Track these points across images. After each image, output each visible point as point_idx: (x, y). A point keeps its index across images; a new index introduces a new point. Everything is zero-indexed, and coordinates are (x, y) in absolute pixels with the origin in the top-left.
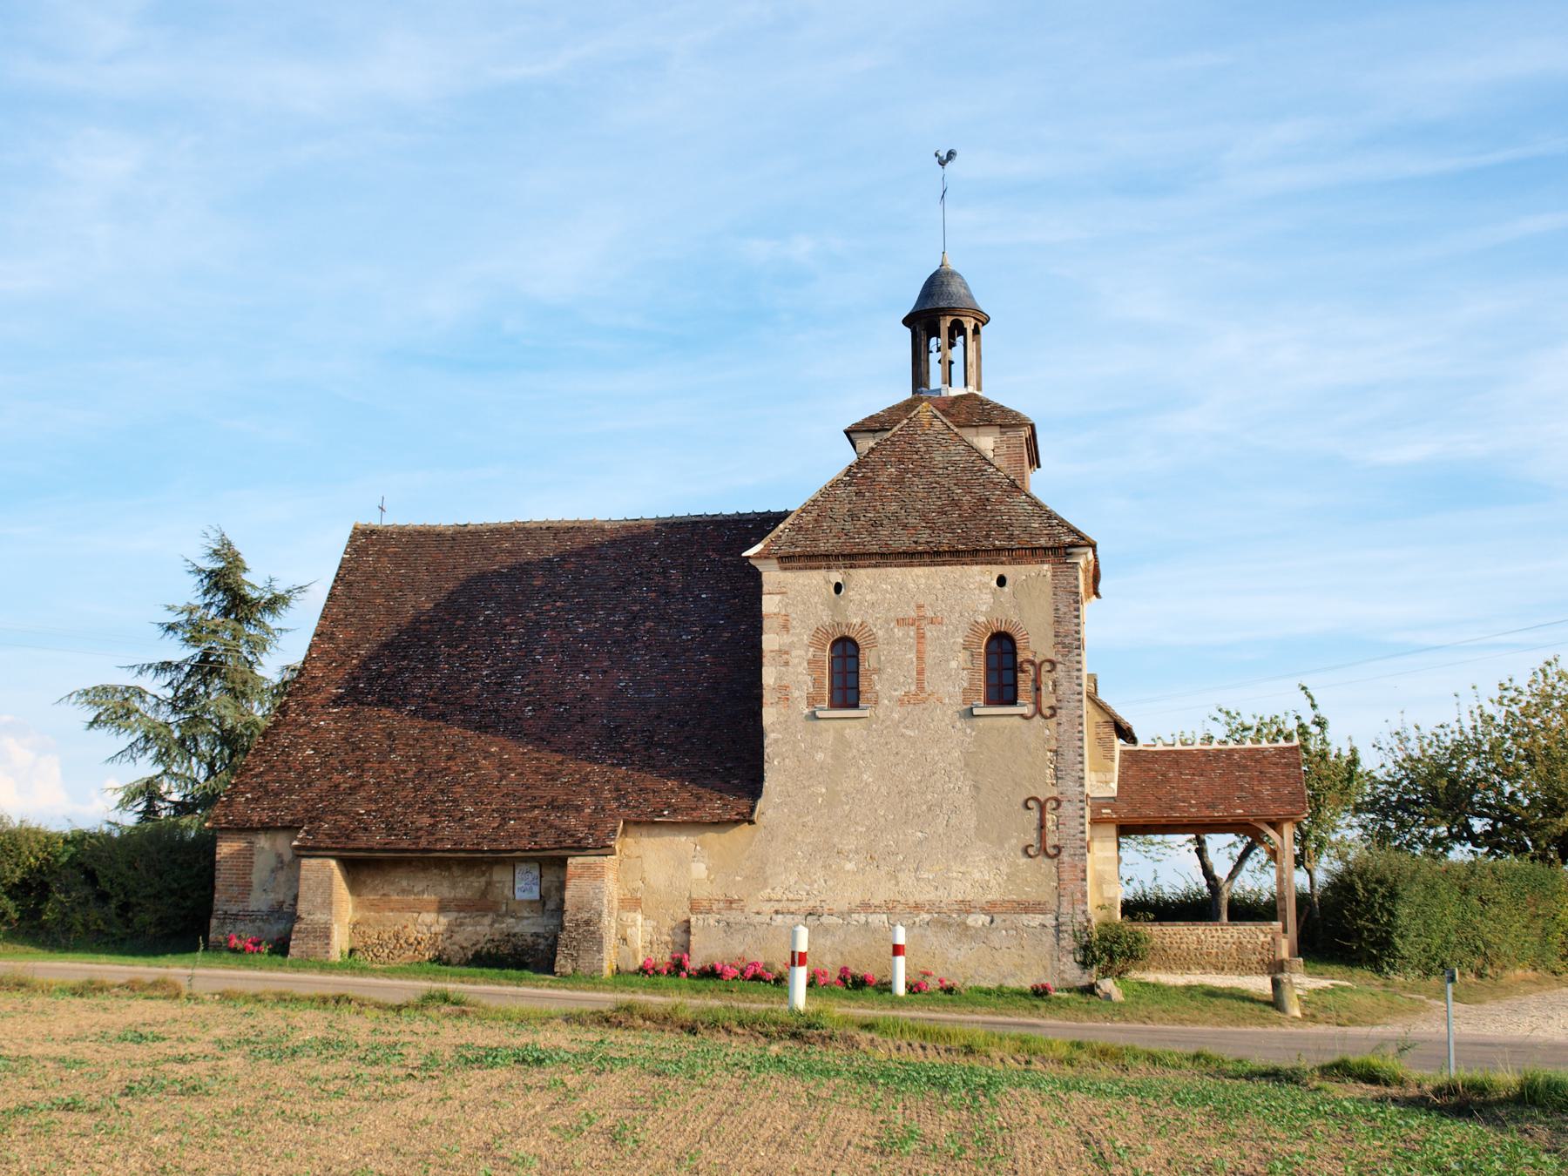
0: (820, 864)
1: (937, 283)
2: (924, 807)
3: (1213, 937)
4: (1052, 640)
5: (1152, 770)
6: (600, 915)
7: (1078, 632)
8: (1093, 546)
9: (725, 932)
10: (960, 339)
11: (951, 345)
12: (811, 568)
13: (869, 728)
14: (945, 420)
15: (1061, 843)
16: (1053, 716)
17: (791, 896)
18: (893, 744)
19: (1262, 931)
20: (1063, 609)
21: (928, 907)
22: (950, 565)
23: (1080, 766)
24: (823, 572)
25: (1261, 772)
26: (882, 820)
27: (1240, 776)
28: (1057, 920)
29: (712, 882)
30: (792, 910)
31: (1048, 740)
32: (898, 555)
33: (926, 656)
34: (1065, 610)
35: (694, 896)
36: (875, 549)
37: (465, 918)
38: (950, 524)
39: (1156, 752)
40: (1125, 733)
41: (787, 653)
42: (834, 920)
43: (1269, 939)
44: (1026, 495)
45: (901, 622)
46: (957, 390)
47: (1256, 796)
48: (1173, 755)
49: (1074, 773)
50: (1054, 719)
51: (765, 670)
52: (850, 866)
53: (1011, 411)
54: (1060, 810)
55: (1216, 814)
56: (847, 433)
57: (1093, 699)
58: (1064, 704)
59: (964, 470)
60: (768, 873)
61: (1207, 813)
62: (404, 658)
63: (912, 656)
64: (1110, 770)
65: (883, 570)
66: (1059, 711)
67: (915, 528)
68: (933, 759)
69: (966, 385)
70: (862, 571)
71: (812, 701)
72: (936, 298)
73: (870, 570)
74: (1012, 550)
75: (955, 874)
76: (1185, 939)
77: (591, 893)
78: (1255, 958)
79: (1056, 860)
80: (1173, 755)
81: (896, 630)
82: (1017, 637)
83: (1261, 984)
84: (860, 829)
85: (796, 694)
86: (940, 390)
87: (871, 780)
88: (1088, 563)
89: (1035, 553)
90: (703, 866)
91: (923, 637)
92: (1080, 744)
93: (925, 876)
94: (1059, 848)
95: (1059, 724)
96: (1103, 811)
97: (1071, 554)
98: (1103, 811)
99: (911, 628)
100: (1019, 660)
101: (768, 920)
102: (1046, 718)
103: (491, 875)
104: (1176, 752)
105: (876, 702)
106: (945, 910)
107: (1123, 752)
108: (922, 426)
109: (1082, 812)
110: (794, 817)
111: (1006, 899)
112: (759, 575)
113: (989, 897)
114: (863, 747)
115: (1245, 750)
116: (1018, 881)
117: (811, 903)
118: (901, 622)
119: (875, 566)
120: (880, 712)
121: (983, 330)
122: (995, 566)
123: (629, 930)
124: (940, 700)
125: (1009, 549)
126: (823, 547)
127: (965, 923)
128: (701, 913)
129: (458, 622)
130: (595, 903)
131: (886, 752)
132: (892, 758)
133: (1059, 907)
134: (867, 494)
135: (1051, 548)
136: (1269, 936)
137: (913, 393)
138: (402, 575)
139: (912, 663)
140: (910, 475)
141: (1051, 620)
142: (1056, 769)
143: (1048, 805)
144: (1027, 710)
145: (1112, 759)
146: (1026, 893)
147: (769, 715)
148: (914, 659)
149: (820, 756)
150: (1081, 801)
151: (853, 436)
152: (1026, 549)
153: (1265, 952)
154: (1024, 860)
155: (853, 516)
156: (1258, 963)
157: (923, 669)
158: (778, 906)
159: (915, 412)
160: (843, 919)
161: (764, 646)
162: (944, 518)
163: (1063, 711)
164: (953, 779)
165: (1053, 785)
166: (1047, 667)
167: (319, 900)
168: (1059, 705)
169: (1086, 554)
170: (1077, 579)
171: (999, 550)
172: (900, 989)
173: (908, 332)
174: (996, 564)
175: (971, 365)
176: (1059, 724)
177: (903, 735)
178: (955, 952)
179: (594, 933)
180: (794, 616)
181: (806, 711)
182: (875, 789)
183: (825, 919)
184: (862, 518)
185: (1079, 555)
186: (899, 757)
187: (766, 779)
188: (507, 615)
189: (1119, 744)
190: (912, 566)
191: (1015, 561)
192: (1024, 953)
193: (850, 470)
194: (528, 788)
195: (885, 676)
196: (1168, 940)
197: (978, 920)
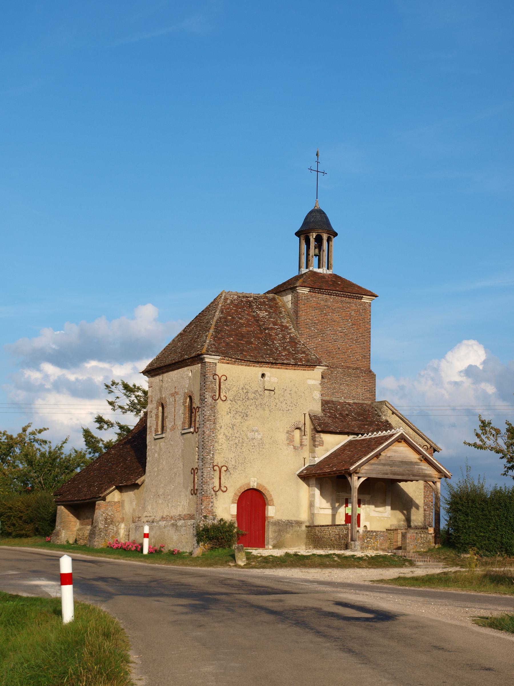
20: (202, 384)
63: (173, 409)
154: (191, 496)
172: (146, 551)
195: (168, 419)
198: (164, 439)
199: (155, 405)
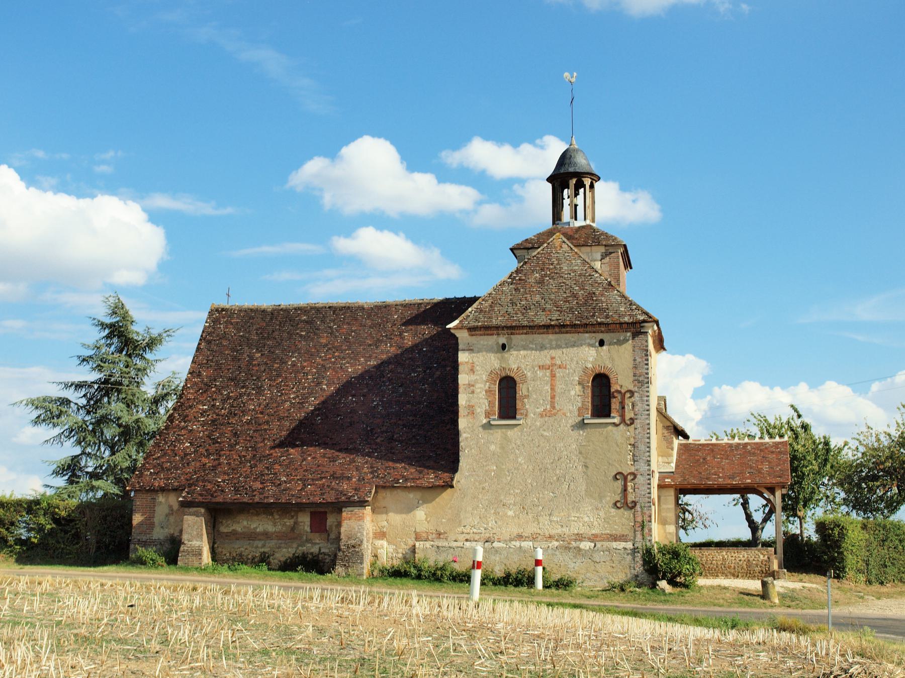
0: (493, 511)
1: (568, 156)
2: (555, 478)
3: (732, 557)
4: (632, 379)
5: (697, 456)
6: (362, 542)
7: (647, 374)
8: (657, 322)
9: (436, 552)
10: (582, 191)
11: (576, 194)
12: (488, 335)
13: (522, 431)
14: (570, 244)
15: (637, 499)
16: (632, 424)
17: (475, 531)
18: (537, 440)
19: (762, 554)
20: (638, 360)
21: (557, 537)
22: (570, 333)
23: (648, 454)
24: (495, 337)
25: (763, 457)
26: (530, 486)
27: (751, 460)
28: (634, 545)
29: (428, 522)
30: (475, 539)
31: (628, 439)
32: (540, 327)
33: (556, 388)
34: (640, 360)
35: (418, 531)
36: (526, 323)
37: (281, 543)
38: (571, 308)
39: (700, 445)
40: (680, 432)
41: (473, 386)
42: (501, 545)
43: (766, 558)
44: (617, 290)
45: (541, 367)
46: (580, 223)
47: (760, 471)
48: (711, 447)
49: (644, 458)
50: (633, 426)
51: (460, 396)
52: (510, 513)
53: (612, 236)
54: (636, 480)
55: (734, 483)
56: (512, 250)
57: (662, 414)
58: (639, 416)
59: (580, 275)
60: (462, 517)
61: (729, 482)
62: (243, 387)
63: (548, 388)
64: (671, 455)
65: (530, 337)
66: (635, 421)
67: (550, 311)
68: (560, 449)
69: (585, 219)
70: (518, 336)
71: (488, 414)
72: (567, 166)
73: (524, 336)
74: (608, 324)
75: (573, 518)
76: (715, 559)
77: (357, 529)
78: (757, 569)
79: (633, 510)
80: (711, 447)
81: (538, 372)
82: (611, 376)
83: (755, 585)
84: (517, 491)
85: (479, 410)
86: (569, 223)
87: (523, 462)
88: (655, 332)
89: (622, 326)
90: (423, 513)
91: (555, 376)
92: (648, 440)
93: (555, 519)
94: (635, 503)
95: (635, 429)
96: (666, 480)
97: (643, 327)
98: (666, 480)
99: (547, 371)
100: (612, 390)
101: (462, 545)
102: (628, 425)
103: (297, 518)
104: (712, 445)
105: (526, 415)
106: (567, 539)
107: (681, 445)
108: (555, 248)
109: (649, 481)
110: (477, 484)
111: (603, 532)
112: (457, 339)
113: (594, 532)
114: (518, 442)
115: (755, 444)
116: (611, 522)
117: (487, 535)
118: (541, 367)
119: (526, 334)
120: (529, 421)
121: (596, 185)
122: (597, 334)
123: (379, 550)
124: (564, 414)
125: (606, 324)
126: (494, 322)
127: (579, 547)
128: (422, 541)
129: (276, 365)
130: (359, 534)
131: (532, 445)
132: (535, 449)
133: (635, 538)
134: (521, 290)
135: (632, 323)
136: (766, 556)
137: (554, 223)
138: (241, 336)
139: (548, 392)
140: (547, 278)
141: (631, 366)
142: (634, 455)
143: (629, 477)
144: (617, 420)
145: (672, 449)
146: (616, 530)
147: (462, 423)
148: (549, 390)
149: (493, 447)
150: (648, 475)
151: (515, 251)
152: (616, 324)
153: (763, 566)
155: (513, 303)
156: (759, 573)
157: (554, 395)
158: (468, 537)
159: (551, 239)
160: (506, 545)
161: (460, 381)
162: (567, 305)
163: (638, 421)
164: (572, 461)
165: (631, 465)
166: (628, 395)
167: (195, 533)
168: (636, 417)
169: (653, 326)
170: (647, 341)
171: (600, 324)
173: (550, 186)
174: (598, 332)
175: (588, 207)
176: (635, 429)
177: (542, 435)
178: (573, 565)
179: (358, 552)
180: (477, 363)
181: (485, 421)
182: (526, 467)
183: (496, 544)
184: (518, 305)
185: (649, 327)
186: (540, 448)
187: (461, 461)
188: (305, 361)
189: (677, 442)
190: (548, 333)
191: (609, 331)
192: (614, 565)
193: (511, 275)
194: (319, 466)
195: (531, 400)
196: (704, 559)
197: (586, 545)
198: (518, 427)
199: (484, 377)
